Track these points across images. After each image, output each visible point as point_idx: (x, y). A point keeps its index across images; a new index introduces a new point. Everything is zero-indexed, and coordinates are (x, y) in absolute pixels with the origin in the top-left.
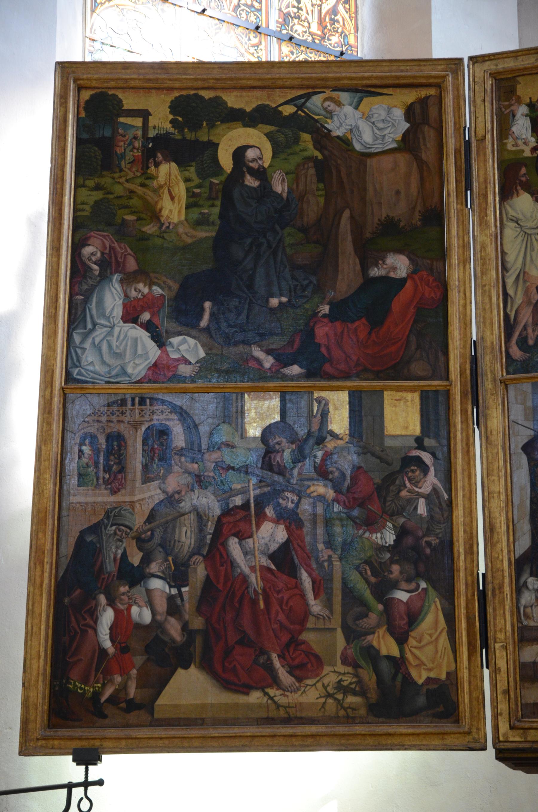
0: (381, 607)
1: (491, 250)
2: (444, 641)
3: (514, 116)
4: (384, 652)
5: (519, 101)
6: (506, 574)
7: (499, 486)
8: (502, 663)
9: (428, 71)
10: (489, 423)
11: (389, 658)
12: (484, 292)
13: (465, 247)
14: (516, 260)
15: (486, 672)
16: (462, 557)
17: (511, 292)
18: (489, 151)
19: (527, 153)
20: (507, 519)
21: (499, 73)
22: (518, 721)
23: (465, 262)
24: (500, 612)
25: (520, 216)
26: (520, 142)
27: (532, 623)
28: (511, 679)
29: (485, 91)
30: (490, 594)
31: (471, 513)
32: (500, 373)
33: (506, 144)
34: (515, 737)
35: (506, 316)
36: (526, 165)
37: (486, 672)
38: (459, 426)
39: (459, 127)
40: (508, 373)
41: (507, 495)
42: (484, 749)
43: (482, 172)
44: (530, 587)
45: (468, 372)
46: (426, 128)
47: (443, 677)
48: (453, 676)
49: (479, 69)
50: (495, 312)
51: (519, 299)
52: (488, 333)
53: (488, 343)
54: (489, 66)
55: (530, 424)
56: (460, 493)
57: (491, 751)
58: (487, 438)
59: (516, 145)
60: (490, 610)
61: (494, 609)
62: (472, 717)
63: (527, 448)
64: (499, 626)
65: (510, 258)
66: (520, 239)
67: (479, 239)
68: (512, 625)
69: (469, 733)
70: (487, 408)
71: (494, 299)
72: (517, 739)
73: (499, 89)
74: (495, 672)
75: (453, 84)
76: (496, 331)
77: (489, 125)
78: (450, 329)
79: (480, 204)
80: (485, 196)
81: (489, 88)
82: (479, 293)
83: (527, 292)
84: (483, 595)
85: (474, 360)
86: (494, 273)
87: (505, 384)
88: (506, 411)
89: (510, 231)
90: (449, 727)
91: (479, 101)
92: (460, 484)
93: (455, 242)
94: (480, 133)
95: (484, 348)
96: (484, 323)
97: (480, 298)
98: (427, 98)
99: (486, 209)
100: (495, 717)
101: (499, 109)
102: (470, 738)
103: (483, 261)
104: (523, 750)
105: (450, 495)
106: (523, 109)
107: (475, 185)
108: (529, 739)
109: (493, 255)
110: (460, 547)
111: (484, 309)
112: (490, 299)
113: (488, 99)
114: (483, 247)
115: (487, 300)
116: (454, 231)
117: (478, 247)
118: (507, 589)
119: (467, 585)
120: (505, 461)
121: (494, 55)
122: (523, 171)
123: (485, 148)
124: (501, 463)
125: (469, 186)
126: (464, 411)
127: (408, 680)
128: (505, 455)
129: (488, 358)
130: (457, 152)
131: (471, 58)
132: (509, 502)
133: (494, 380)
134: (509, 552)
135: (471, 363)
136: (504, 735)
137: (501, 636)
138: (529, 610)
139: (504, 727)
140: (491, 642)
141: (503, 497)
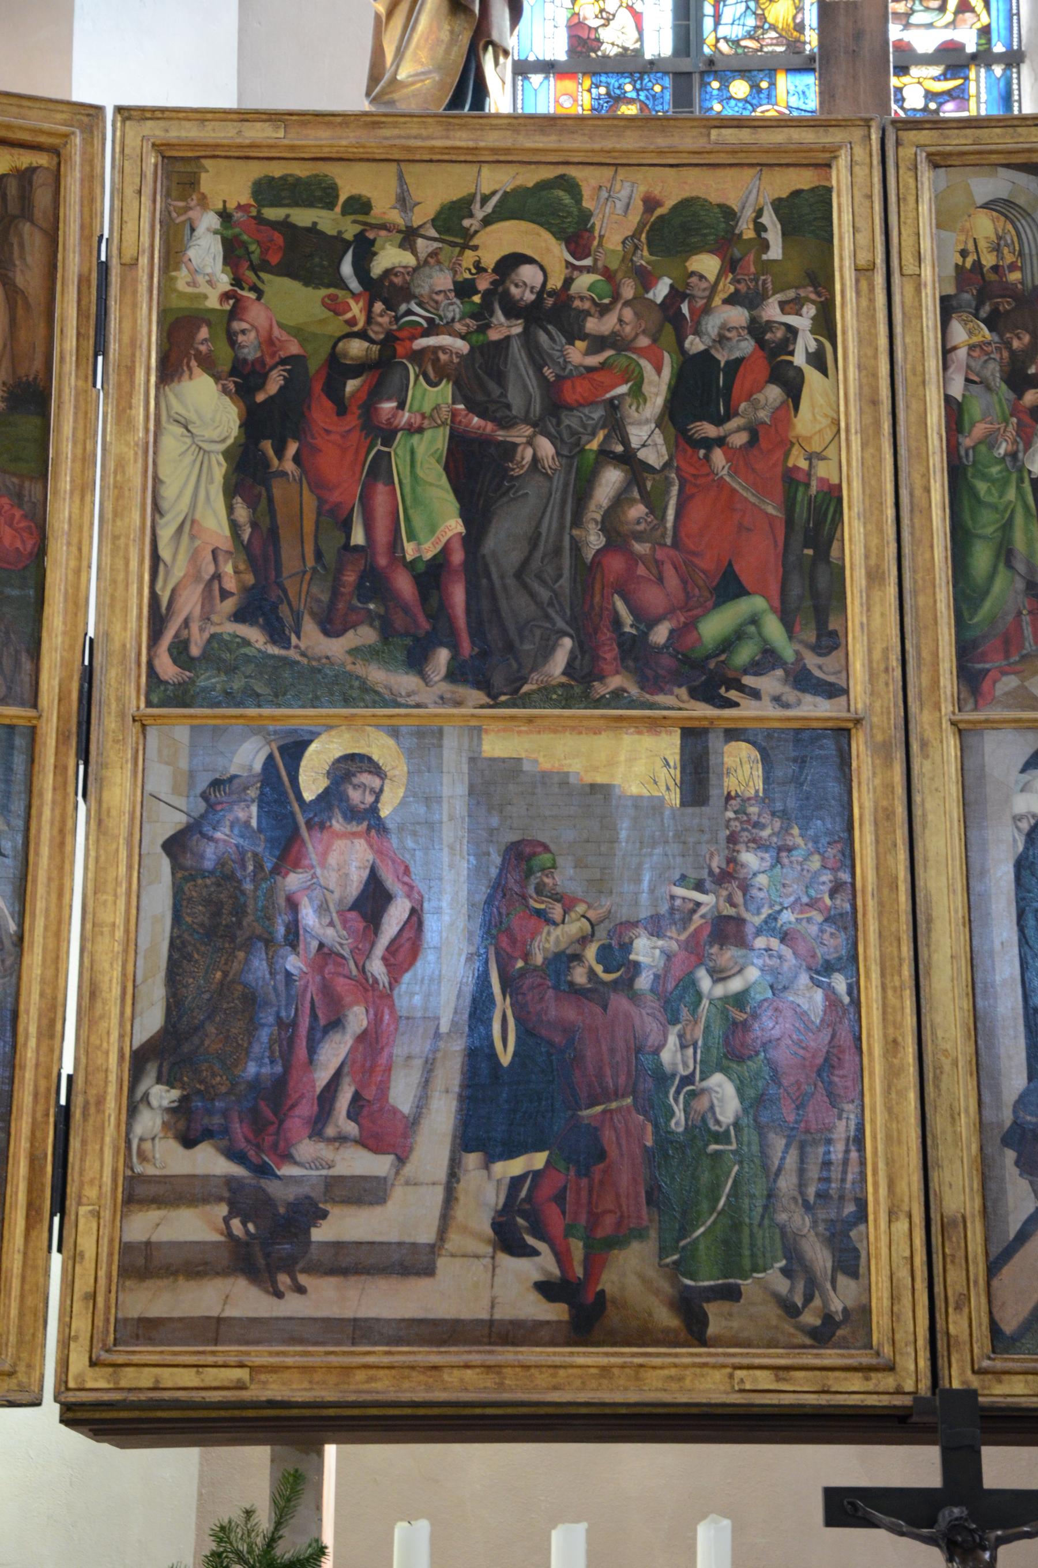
1: (134, 472)
3: (193, 230)
5: (204, 203)
6: (113, 1077)
7: (115, 914)
8: (87, 1244)
9: (36, 120)
10: (106, 795)
12: (115, 549)
13: (86, 460)
14: (179, 496)
15: (56, 1260)
16: (32, 1043)
17: (165, 553)
18: (143, 287)
19: (213, 302)
20: (124, 974)
21: (169, 145)
22: (108, 1351)
23: (84, 488)
24: (93, 1147)
25: (192, 416)
26: (201, 279)
27: (150, 1170)
28: (102, 1273)
29: (142, 175)
30: (77, 1114)
31: (56, 960)
32: (135, 702)
33: (173, 279)
34: (98, 1381)
35: (154, 597)
36: (209, 324)
37: (56, 1260)
38: (48, 796)
39: (91, 237)
40: (149, 704)
41: (127, 931)
42: (37, 1403)
43: (127, 325)
44: (154, 1102)
45: (75, 696)
46: (26, 228)
49: (135, 132)
50: (134, 588)
51: (179, 569)
52: (118, 627)
53: (117, 645)
54: (154, 130)
55: (181, 802)
56: (40, 923)
57: (51, 1409)
58: (100, 822)
59: (194, 284)
60: (75, 1144)
61: (84, 1143)
62: (20, 1342)
63: (174, 846)
64: (89, 1174)
65: (169, 492)
66: (189, 458)
67: (114, 450)
68: (115, 1173)
70: (104, 765)
71: (134, 565)
72: (102, 1384)
73: (168, 175)
74: (73, 1259)
75: (84, 153)
76: (133, 624)
77: (145, 239)
78: (47, 611)
79: (119, 386)
80: (131, 371)
81: (149, 171)
82: (107, 549)
83: (194, 557)
84: (65, 1115)
85: (88, 675)
86: (136, 516)
87: (142, 724)
88: (140, 772)
89: (173, 441)
91: (129, 192)
92: (40, 905)
93: (68, 449)
94: (129, 254)
95: (108, 654)
96: (112, 606)
97: (107, 560)
98: (32, 170)
99: (130, 395)
100: (65, 1343)
101: (167, 212)
102: (13, 1383)
103: (117, 491)
104: (109, 1405)
105: (21, 925)
106: (208, 221)
107: (113, 347)
108: (123, 1384)
109: (138, 481)
110: (30, 1024)
111: (114, 582)
112: (127, 564)
113: (147, 190)
114: (121, 465)
115: (120, 564)
116: (67, 428)
117: (111, 465)
118: (111, 1104)
119: (36, 1096)
120: (130, 867)
121: (163, 110)
122: (204, 333)
123: (135, 281)
124: (122, 869)
125: (101, 348)
126: (60, 769)
128: (130, 856)
129: (113, 673)
130: (83, 281)
131: (119, 109)
132: (131, 944)
133: (122, 715)
134: (121, 1036)
135: (82, 679)
136: (80, 1377)
137: (91, 1193)
138: (147, 1146)
139: (78, 1361)
140: (71, 1203)
141: (119, 934)
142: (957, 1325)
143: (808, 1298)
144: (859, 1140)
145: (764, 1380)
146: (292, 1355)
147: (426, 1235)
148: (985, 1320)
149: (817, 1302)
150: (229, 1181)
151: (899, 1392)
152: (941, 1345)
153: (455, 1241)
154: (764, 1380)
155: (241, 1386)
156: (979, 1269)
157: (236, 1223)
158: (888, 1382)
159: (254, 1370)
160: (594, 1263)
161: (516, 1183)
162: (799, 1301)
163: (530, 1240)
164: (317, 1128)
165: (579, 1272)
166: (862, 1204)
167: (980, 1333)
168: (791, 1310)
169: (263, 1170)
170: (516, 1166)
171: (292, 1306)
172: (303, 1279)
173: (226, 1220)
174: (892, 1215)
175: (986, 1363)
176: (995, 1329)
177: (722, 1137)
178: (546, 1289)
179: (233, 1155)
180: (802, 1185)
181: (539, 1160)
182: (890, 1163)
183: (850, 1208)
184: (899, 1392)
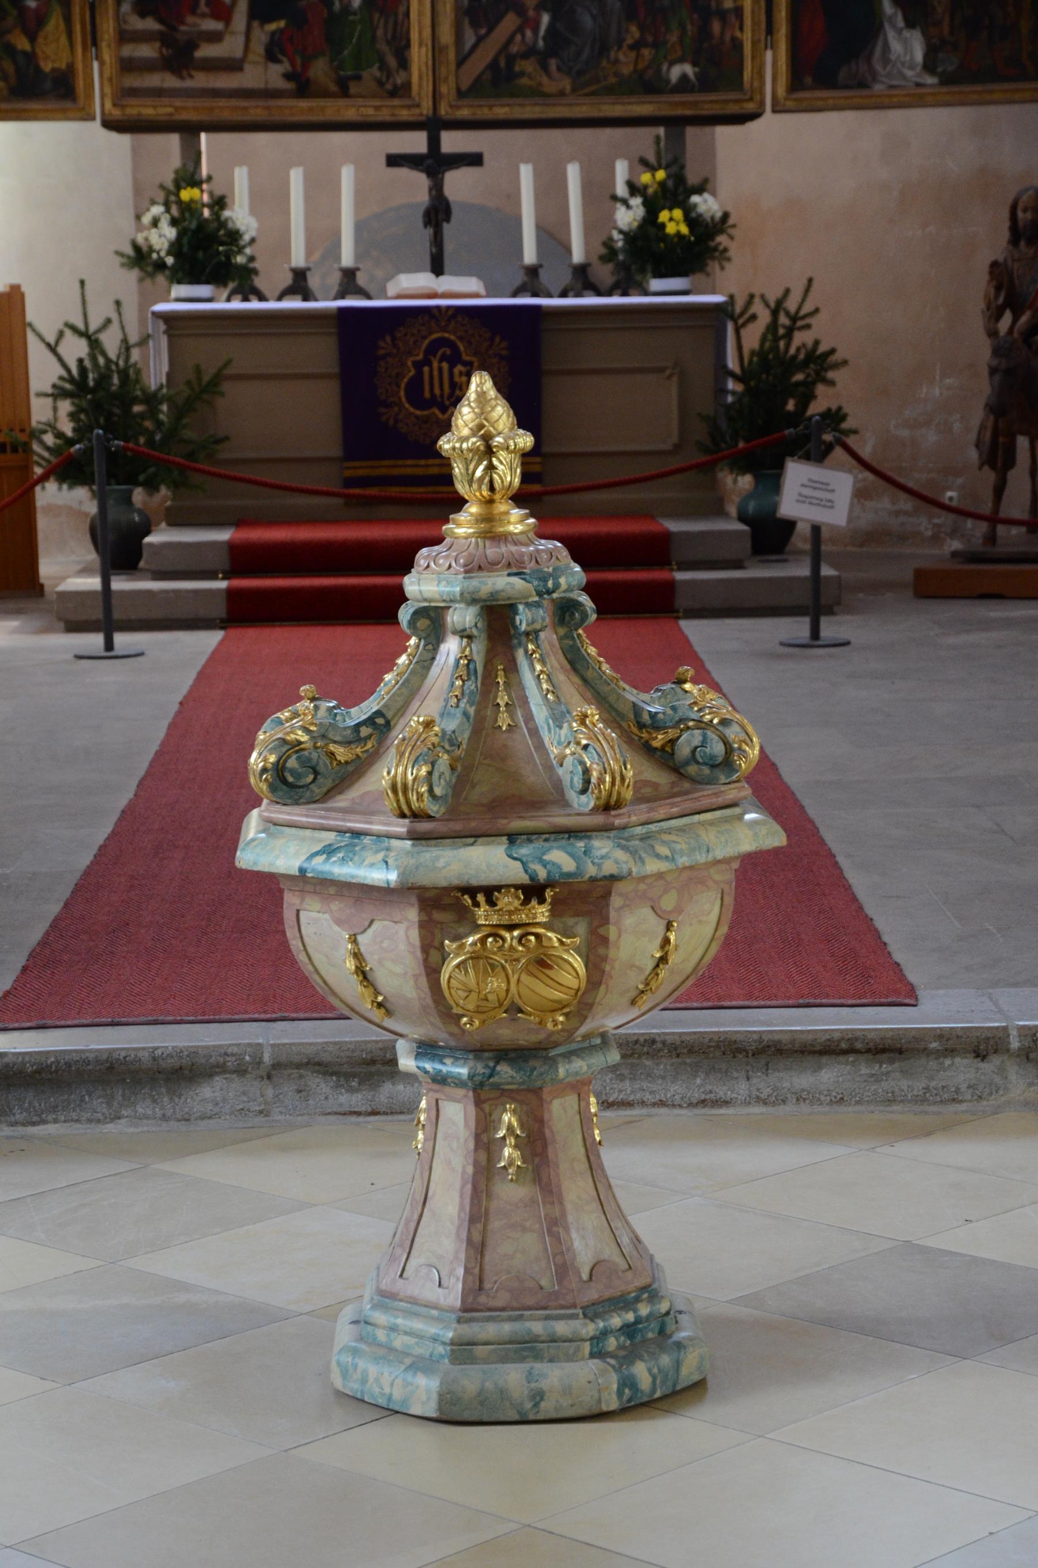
0: (15, 12)
2: (64, 40)
4: (19, 47)
11: (24, 53)
15: (96, 65)
34: (117, 113)
37: (96, 65)
47: (64, 66)
48: (71, 68)
60: (98, 18)
69: (83, 109)
74: (102, 64)
90: (69, 104)
100: (103, 96)
127: (38, 70)
139: (108, 105)
142: (444, 89)
143: (388, 78)
144: (407, 14)
145: (371, 111)
146: (190, 103)
147: (239, 53)
148: (454, 86)
149: (391, 81)
150: (160, 33)
151: (421, 115)
152: (437, 96)
153: (251, 57)
154: (371, 111)
155: (171, 114)
156: (453, 66)
157: (164, 51)
158: (417, 111)
159: (176, 109)
160: (305, 66)
161: (273, 34)
162: (384, 79)
163: (280, 57)
164: (193, 11)
165: (299, 69)
166: (408, 41)
167: (454, 91)
168: (380, 83)
169: (174, 29)
170: (273, 27)
171: (189, 83)
172: (193, 73)
173: (160, 49)
174: (420, 45)
175: (454, 103)
176: (458, 90)
177: (355, 14)
178: (287, 76)
179: (161, 21)
180: (385, 34)
181: (282, 24)
182: (420, 23)
183: (404, 42)
184: (421, 115)
